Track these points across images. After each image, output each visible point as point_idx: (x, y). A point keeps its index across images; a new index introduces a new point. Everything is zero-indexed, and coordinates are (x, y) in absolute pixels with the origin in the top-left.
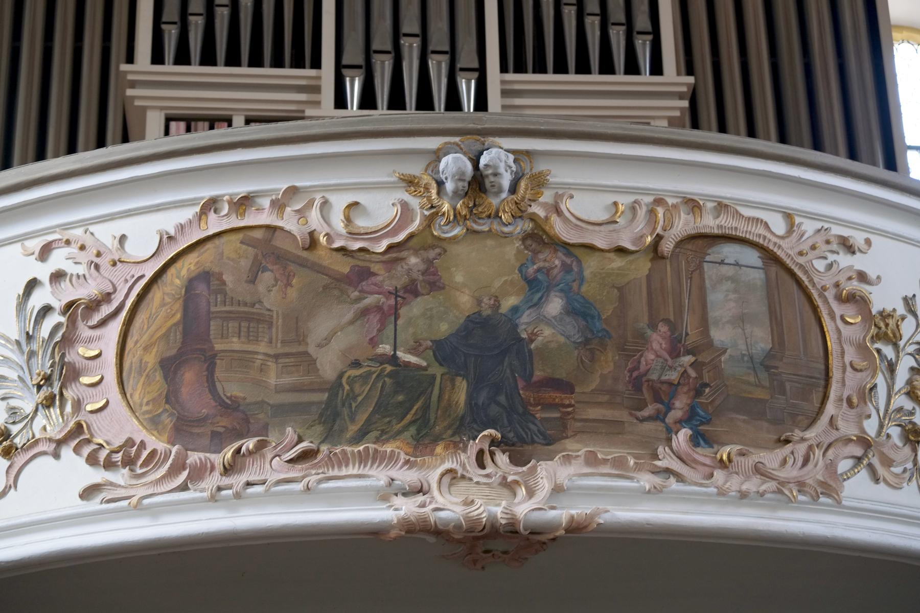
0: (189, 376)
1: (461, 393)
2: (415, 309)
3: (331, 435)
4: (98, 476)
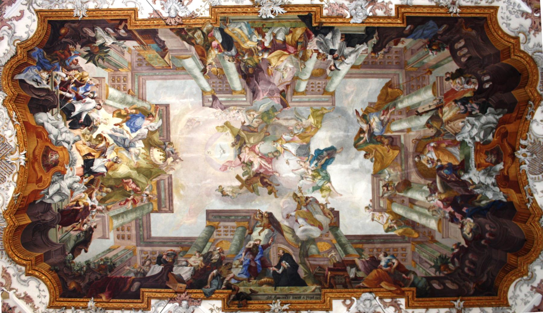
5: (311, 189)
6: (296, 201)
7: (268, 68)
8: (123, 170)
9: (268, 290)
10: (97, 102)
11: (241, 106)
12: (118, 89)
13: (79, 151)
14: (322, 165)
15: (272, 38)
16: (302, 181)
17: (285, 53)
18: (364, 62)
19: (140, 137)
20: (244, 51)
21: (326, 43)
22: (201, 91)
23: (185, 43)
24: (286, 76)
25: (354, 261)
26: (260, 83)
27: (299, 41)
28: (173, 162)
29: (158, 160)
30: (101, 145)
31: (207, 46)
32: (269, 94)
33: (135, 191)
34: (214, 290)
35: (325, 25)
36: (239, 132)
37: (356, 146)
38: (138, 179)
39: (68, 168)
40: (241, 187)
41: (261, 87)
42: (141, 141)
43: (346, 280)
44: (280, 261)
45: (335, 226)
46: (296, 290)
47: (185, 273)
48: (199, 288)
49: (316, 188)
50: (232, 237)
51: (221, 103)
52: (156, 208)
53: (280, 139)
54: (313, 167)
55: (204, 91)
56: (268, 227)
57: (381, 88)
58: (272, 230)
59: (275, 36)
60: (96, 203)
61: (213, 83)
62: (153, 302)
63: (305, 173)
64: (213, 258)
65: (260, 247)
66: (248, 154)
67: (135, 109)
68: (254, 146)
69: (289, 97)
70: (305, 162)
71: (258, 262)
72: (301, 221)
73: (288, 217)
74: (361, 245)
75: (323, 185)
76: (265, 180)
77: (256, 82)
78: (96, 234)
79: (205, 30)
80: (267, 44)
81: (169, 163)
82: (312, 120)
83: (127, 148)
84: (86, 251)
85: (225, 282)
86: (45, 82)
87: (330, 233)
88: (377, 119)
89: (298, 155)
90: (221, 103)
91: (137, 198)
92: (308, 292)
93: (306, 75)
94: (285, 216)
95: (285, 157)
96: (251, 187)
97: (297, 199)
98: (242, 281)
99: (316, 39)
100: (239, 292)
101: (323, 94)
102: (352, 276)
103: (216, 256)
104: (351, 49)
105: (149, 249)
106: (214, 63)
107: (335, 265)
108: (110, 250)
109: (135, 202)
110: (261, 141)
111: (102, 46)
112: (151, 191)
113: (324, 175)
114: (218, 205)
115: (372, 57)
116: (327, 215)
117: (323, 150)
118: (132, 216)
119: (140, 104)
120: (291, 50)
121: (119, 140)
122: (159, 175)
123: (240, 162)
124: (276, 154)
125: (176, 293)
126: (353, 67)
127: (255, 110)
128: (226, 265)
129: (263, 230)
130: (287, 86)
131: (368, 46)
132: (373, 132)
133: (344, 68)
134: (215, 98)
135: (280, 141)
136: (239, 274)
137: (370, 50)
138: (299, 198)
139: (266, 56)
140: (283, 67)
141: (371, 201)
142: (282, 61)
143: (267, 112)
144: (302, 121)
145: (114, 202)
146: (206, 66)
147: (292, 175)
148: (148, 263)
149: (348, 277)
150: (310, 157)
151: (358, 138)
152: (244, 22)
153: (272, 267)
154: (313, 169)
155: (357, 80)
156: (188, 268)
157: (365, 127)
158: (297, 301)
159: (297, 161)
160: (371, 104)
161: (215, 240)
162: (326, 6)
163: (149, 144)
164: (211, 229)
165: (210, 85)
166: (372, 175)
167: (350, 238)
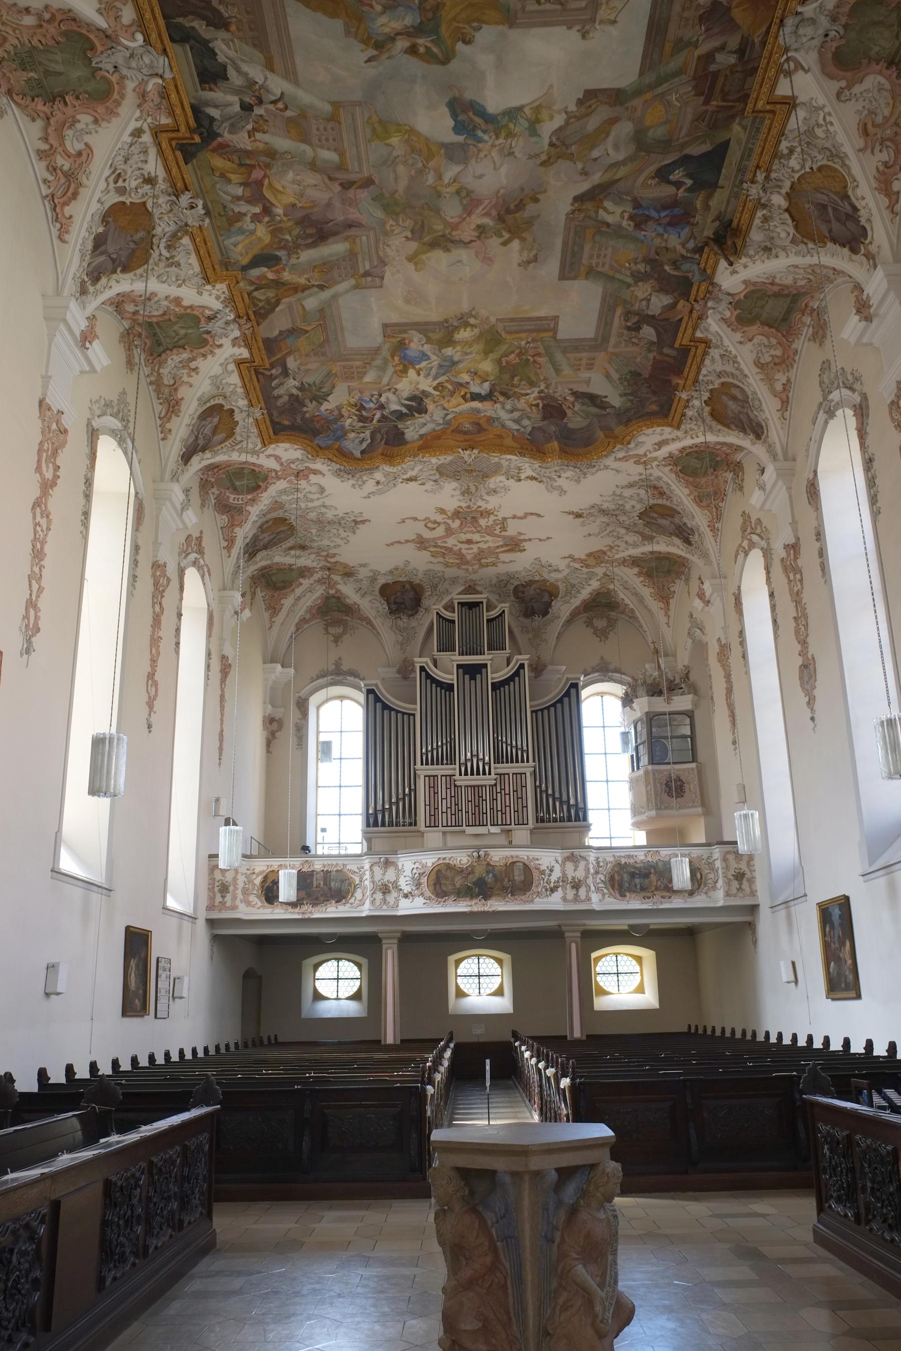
0: (438, 886)
1: (477, 890)
2: (470, 876)
3: (458, 897)
4: (425, 901)
5: (533, 139)
6: (556, 162)
7: (301, 207)
8: (487, 366)
9: (718, 200)
10: (385, 391)
11: (377, 241)
12: (365, 373)
13: (458, 405)
14: (486, 122)
15: (242, 203)
16: (516, 154)
17: (266, 182)
18: (255, 46)
19: (437, 352)
20: (276, 240)
21: (230, 118)
22: (357, 291)
23: (278, 309)
24: (313, 182)
25: (699, 57)
26: (331, 218)
27: (237, 161)
28: (476, 318)
29: (473, 333)
30: (450, 387)
31: (278, 284)
32: (350, 205)
33: (519, 355)
34: (700, 269)
35: (192, 122)
36: (424, 244)
37: (445, 60)
38: (502, 352)
39: (482, 415)
40: (523, 240)
41: (338, 215)
42: (443, 351)
43: (737, 71)
44: (669, 182)
45: (616, 97)
46: (733, 156)
47: (658, 303)
48: (691, 285)
49: (533, 129)
50: (610, 249)
51: (375, 267)
52: (551, 334)
53: (435, 188)
54: (490, 137)
55: (357, 287)
56: (601, 201)
57: (308, 11)
58: (605, 197)
59: (239, 199)
60: (536, 390)
61: (340, 276)
62: (699, 334)
63: (501, 150)
64: (643, 270)
65: (635, 211)
66: (463, 232)
67: (393, 357)
68: (446, 223)
69: (353, 177)
70: (480, 151)
71: (663, 214)
72: (595, 153)
73: (585, 173)
74: (667, 44)
75: (527, 120)
76: (512, 206)
77: (331, 224)
78: (583, 388)
79: (252, 288)
80: (257, 210)
81: (477, 322)
82: (395, 140)
83: (454, 363)
84: (606, 397)
85: (689, 255)
86: (362, 435)
87: (628, 104)
88: (383, 20)
89: (465, 161)
90: (375, 267)
91: (531, 352)
92: (743, 136)
93: (304, 151)
94: (584, 177)
95: (468, 181)
96: (523, 226)
97: (551, 161)
98: (693, 233)
99: (227, 135)
100: (712, 236)
101: (340, 123)
102: (732, 59)
103: (641, 267)
104: (231, 73)
105: (613, 341)
106: (306, 276)
107: (698, 94)
108: (608, 376)
109: (539, 354)
110: (440, 215)
111: (301, 388)
112: (522, 339)
113: (507, 118)
114: (552, 267)
115: (238, 29)
116: (589, 110)
117: (455, 120)
118: (559, 357)
119: (385, 352)
120: (257, 174)
121: (442, 371)
122: (497, 332)
123: (478, 244)
124: (463, 194)
125: (691, 312)
126: (270, 66)
127: (383, 223)
128: (658, 254)
129: (605, 210)
130: (331, 179)
131: (216, 39)
132: (412, 26)
133: (277, 85)
134: (366, 274)
135: (439, 188)
136: (679, 237)
137: (222, 34)
138: (549, 158)
139: (279, 211)
140: (296, 186)
141: (570, 28)
142: (284, 187)
143: (386, 208)
144: (398, 156)
145: (537, 374)
146: (313, 286)
147: (504, 170)
148: (634, 340)
149: (734, 65)
150: (470, 142)
151: (429, 57)
152: (223, 241)
153: (677, 195)
154: (494, 137)
155: (298, 60)
156: (654, 299)
157: (402, 44)
158: (755, 156)
159: (477, 162)
160: (348, 33)
161: (611, 267)
162: (149, 120)
163: (448, 341)
164: (591, 273)
165: (343, 281)
166: (511, 27)
167: (648, 62)
